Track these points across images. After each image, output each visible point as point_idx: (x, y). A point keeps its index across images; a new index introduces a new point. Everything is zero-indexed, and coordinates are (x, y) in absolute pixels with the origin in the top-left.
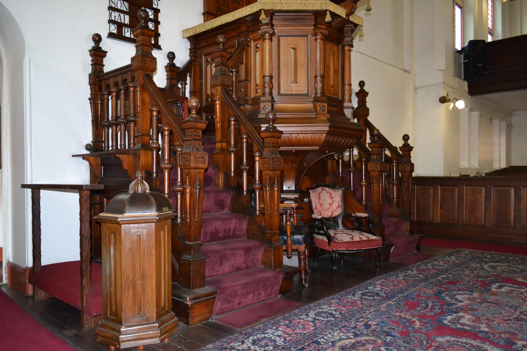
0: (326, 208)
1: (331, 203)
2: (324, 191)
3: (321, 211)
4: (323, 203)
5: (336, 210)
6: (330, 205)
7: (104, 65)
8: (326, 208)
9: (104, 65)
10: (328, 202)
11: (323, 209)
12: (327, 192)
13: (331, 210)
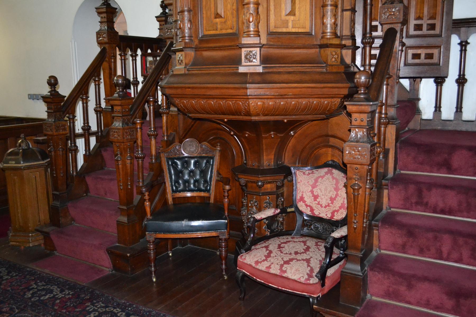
0: (324, 203)
1: (333, 197)
2: (329, 176)
3: (314, 205)
4: (320, 194)
5: (337, 211)
6: (332, 200)
7: (356, 11)
8: (324, 203)
9: (356, 11)
10: (330, 195)
11: (319, 204)
12: (333, 178)
13: (332, 209)
